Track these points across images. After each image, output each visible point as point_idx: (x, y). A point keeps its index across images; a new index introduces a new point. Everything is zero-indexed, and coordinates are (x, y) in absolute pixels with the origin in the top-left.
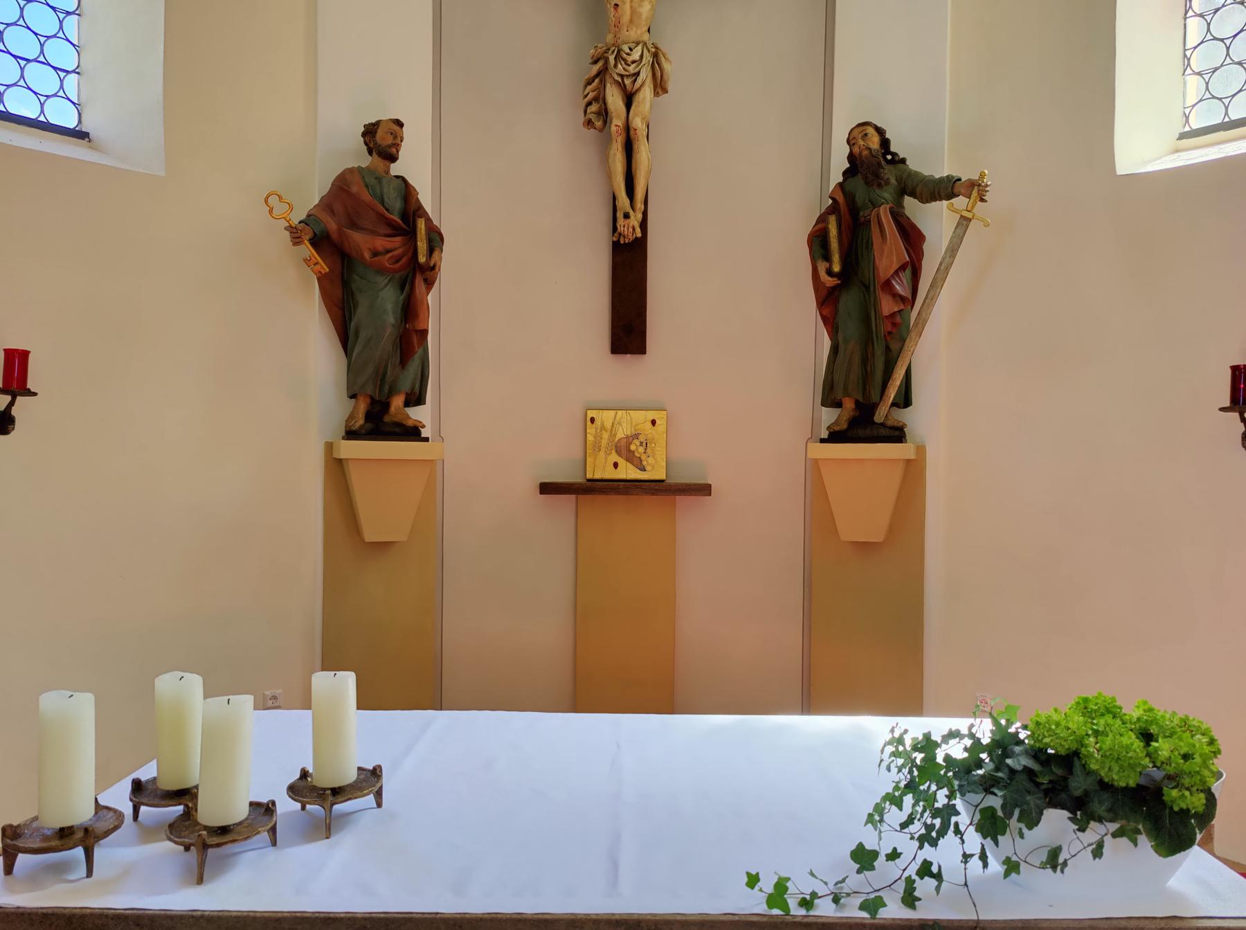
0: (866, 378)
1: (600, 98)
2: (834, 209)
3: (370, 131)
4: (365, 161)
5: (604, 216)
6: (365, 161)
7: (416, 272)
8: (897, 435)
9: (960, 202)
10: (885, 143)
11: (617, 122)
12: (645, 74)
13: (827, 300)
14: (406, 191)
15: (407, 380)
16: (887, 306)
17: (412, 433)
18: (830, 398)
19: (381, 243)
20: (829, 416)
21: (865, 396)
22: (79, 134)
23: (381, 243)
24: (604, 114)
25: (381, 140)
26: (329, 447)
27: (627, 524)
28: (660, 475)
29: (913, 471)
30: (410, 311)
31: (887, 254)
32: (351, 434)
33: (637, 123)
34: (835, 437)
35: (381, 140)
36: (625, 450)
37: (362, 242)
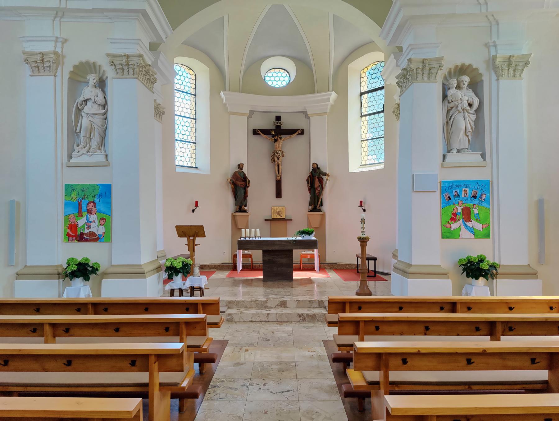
0: (315, 202)
1: (274, 158)
2: (310, 176)
3: (239, 165)
4: (238, 170)
6: (238, 170)
7: (246, 187)
8: (320, 211)
9: (326, 177)
10: (317, 166)
11: (276, 162)
12: (281, 155)
13: (309, 190)
14: (244, 174)
15: (244, 203)
16: (317, 192)
17: (245, 211)
18: (310, 205)
19: (241, 183)
20: (310, 207)
21: (316, 204)
23: (241, 183)
24: (274, 161)
25: (240, 166)
26: (232, 214)
29: (323, 216)
30: (246, 193)
31: (317, 184)
32: (237, 212)
33: (280, 162)
34: (311, 211)
35: (240, 166)
36: (278, 214)
37: (239, 183)
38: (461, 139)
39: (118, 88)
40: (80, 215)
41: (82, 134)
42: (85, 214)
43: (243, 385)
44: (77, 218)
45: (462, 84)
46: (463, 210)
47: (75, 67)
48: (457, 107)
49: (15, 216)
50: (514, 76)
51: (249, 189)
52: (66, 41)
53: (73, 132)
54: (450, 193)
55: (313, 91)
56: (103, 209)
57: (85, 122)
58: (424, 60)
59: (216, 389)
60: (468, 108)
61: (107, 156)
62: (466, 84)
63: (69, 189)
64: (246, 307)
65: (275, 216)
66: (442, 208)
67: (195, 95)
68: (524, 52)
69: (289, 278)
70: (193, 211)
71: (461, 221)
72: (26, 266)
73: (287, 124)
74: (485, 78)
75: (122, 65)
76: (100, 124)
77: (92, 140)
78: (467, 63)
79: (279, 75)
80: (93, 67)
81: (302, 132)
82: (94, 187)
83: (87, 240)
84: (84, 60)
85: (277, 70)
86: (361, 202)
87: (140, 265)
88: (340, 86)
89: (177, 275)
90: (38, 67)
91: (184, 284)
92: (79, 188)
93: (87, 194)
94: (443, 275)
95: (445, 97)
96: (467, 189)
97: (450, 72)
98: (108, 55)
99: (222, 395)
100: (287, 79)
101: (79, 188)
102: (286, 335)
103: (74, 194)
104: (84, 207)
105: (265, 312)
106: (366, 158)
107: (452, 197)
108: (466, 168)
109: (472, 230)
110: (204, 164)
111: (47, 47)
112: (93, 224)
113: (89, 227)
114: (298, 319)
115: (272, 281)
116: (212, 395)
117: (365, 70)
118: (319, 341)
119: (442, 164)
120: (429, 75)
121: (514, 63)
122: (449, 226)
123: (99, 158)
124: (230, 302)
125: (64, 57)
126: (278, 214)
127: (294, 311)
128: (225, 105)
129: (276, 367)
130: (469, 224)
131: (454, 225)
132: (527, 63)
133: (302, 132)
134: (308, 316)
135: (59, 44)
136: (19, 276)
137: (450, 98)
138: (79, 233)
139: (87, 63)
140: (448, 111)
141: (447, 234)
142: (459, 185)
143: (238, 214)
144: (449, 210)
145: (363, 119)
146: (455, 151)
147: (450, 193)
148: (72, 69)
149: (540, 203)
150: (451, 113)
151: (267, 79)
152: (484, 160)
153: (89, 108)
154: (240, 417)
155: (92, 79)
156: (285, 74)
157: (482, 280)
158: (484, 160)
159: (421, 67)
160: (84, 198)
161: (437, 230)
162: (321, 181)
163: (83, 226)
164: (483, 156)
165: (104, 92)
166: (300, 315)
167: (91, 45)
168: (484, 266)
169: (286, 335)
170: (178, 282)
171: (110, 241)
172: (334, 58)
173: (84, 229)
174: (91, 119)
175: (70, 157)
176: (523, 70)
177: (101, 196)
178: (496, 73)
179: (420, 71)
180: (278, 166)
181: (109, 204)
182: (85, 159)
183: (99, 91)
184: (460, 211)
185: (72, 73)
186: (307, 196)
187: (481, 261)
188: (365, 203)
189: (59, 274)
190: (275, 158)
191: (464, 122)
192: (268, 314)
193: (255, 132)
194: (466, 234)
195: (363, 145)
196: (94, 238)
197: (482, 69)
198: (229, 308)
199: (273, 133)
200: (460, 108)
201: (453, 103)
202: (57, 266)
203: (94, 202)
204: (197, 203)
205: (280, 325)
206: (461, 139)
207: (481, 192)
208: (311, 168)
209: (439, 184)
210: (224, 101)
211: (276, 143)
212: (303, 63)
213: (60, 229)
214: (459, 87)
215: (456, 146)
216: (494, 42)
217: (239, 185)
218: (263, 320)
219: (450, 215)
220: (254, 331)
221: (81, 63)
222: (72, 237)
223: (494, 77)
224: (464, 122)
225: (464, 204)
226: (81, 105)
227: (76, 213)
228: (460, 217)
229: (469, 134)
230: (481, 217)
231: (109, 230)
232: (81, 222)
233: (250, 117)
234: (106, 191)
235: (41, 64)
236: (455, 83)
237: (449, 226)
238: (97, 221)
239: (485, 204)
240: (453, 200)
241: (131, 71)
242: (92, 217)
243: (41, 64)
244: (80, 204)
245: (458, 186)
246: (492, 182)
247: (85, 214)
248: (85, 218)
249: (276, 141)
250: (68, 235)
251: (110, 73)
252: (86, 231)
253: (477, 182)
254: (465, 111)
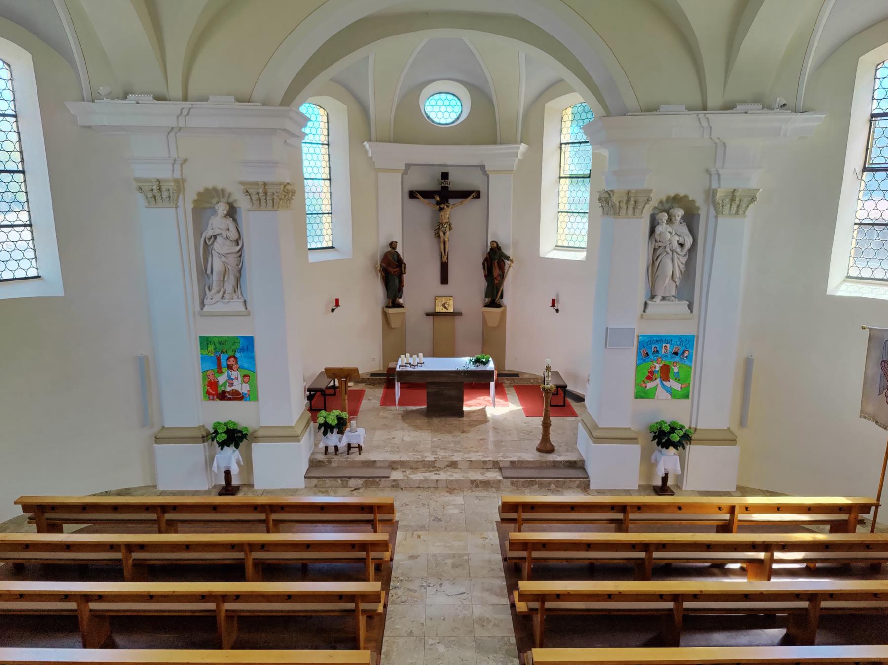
1: (438, 233)
2: (486, 260)
5: (439, 258)
6: (390, 249)
8: (499, 306)
16: (496, 282)
17: (400, 306)
18: (486, 297)
20: (487, 300)
21: (494, 296)
22: (332, 248)
24: (439, 236)
25: (393, 245)
27: (443, 322)
28: (452, 310)
29: (504, 313)
31: (496, 272)
32: (388, 307)
34: (486, 306)
35: (393, 245)
37: (391, 270)
38: (667, 286)
39: (253, 221)
40: (220, 371)
41: (215, 277)
42: (225, 370)
43: (422, 586)
44: (216, 375)
45: (673, 218)
46: (661, 368)
47: (199, 194)
48: (665, 247)
49: (145, 372)
50: (737, 213)
51: (404, 276)
52: (185, 161)
53: (204, 272)
54: (648, 348)
55: (494, 140)
56: (245, 365)
57: (217, 265)
58: (629, 192)
59: (397, 590)
60: (679, 250)
61: (245, 301)
62: (678, 219)
63: (205, 342)
64: (412, 468)
65: (439, 309)
66: (637, 365)
67: (328, 145)
68: (753, 185)
69: (460, 413)
70: (333, 310)
71: (658, 380)
72: (163, 427)
73: (457, 181)
74: (702, 213)
75: (258, 194)
76: (235, 263)
77: (226, 284)
78: (682, 194)
79: (447, 103)
80: (220, 193)
81: (478, 195)
82: (234, 340)
83: (229, 399)
84: (210, 187)
85: (443, 96)
86: (553, 301)
87: (292, 427)
88: (532, 135)
89: (332, 432)
90: (155, 197)
91: (340, 440)
92: (216, 340)
93: (226, 347)
94: (633, 440)
95: (652, 231)
96: (668, 345)
97: (661, 202)
98: (242, 183)
99: (404, 599)
100: (458, 110)
101: (216, 340)
102: (456, 511)
103: (211, 347)
104: (224, 363)
105: (433, 476)
106: (563, 237)
107: (650, 354)
108: (669, 320)
109: (670, 391)
110: (345, 244)
111: (165, 173)
112: (235, 381)
113: (231, 385)
114: (469, 485)
115: (439, 416)
116: (395, 598)
117: (569, 111)
118: (492, 522)
119: (642, 315)
120: (634, 208)
121: (737, 199)
122: (644, 385)
123: (237, 306)
124: (394, 462)
125: (184, 181)
126: (444, 305)
127: (465, 475)
128: (371, 158)
129: (450, 561)
130: (665, 383)
131: (650, 385)
132: (753, 199)
133: (478, 195)
134: (481, 482)
135: (177, 166)
136: (158, 439)
138: (220, 391)
139: (215, 190)
140: (654, 249)
141: (642, 394)
142: (659, 340)
143: (391, 310)
144: (646, 367)
145: (562, 180)
146: (658, 299)
147: (648, 348)
148: (196, 197)
149: (748, 364)
150: (658, 253)
151: (428, 109)
152: (691, 312)
153: (221, 247)
154: (423, 624)
155: (222, 208)
156: (455, 101)
157: (672, 450)
158: (691, 312)
159: (625, 198)
160: (223, 352)
161: (630, 387)
162: (502, 267)
163: (225, 383)
164: (690, 307)
165: (235, 220)
166: (472, 482)
167: (217, 167)
168: (675, 437)
169: (456, 511)
170: (333, 439)
171: (257, 400)
172: (524, 94)
173: (225, 387)
174: (223, 259)
175: (203, 305)
176: (748, 206)
177: (242, 350)
178: (716, 209)
179: (623, 205)
180: (444, 243)
181: (252, 359)
182: (220, 307)
183: (229, 221)
184: (658, 369)
185: (195, 201)
186: (483, 284)
187: (673, 430)
188: (558, 301)
189: (203, 437)
190: (439, 230)
191: (673, 266)
192: (437, 480)
193: (413, 195)
194: (661, 394)
195: (561, 219)
196: (237, 396)
197: (700, 202)
198: (393, 469)
199: (438, 199)
200: (668, 250)
202: (199, 428)
203: (234, 357)
204: (337, 301)
205: (451, 493)
206: (667, 286)
207: (683, 348)
208: (489, 247)
209: (636, 338)
210: (370, 155)
211: (443, 213)
212: (482, 98)
213: (198, 387)
214: (670, 221)
215: (660, 293)
216: (717, 170)
217: (392, 270)
218: (432, 485)
219: (647, 373)
220: (424, 505)
221: (207, 190)
222: (213, 395)
223: (713, 212)
224: (673, 266)
225: (663, 360)
226: (209, 239)
227: (215, 367)
228: (658, 375)
229: (677, 280)
230: (681, 375)
231: (254, 388)
232: (222, 379)
233: (405, 173)
234: (248, 345)
235: (158, 193)
236: (665, 217)
237: (644, 385)
238: (240, 379)
239: (687, 362)
240: (651, 356)
241: (270, 202)
242: (234, 374)
243: (158, 193)
244: (219, 359)
245: (657, 341)
246: (697, 337)
247: (225, 370)
248: (226, 375)
249: (441, 209)
250: (208, 393)
251: (243, 203)
252: (228, 389)
253: (680, 337)
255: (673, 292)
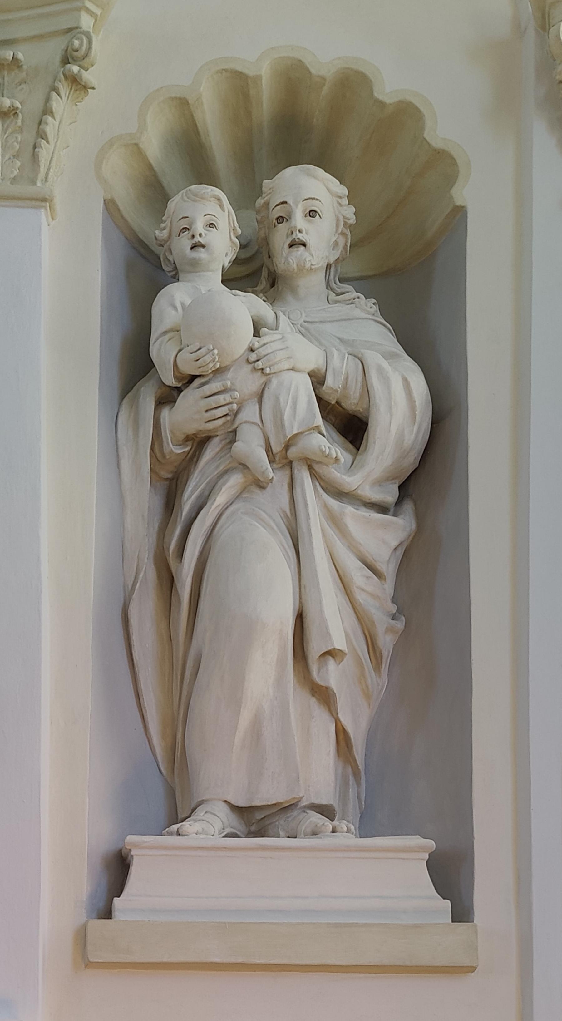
38: (267, 722)
48: (232, 436)
137: (162, 352)
146: (208, 826)
152: (462, 913)
158: (462, 913)
164: (450, 875)
200: (251, 446)
201: (189, 399)
206: (267, 722)
229: (333, 676)
236: (213, 224)
254: (304, 478)
255: (320, 776)
